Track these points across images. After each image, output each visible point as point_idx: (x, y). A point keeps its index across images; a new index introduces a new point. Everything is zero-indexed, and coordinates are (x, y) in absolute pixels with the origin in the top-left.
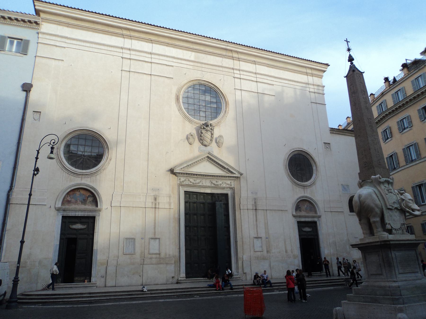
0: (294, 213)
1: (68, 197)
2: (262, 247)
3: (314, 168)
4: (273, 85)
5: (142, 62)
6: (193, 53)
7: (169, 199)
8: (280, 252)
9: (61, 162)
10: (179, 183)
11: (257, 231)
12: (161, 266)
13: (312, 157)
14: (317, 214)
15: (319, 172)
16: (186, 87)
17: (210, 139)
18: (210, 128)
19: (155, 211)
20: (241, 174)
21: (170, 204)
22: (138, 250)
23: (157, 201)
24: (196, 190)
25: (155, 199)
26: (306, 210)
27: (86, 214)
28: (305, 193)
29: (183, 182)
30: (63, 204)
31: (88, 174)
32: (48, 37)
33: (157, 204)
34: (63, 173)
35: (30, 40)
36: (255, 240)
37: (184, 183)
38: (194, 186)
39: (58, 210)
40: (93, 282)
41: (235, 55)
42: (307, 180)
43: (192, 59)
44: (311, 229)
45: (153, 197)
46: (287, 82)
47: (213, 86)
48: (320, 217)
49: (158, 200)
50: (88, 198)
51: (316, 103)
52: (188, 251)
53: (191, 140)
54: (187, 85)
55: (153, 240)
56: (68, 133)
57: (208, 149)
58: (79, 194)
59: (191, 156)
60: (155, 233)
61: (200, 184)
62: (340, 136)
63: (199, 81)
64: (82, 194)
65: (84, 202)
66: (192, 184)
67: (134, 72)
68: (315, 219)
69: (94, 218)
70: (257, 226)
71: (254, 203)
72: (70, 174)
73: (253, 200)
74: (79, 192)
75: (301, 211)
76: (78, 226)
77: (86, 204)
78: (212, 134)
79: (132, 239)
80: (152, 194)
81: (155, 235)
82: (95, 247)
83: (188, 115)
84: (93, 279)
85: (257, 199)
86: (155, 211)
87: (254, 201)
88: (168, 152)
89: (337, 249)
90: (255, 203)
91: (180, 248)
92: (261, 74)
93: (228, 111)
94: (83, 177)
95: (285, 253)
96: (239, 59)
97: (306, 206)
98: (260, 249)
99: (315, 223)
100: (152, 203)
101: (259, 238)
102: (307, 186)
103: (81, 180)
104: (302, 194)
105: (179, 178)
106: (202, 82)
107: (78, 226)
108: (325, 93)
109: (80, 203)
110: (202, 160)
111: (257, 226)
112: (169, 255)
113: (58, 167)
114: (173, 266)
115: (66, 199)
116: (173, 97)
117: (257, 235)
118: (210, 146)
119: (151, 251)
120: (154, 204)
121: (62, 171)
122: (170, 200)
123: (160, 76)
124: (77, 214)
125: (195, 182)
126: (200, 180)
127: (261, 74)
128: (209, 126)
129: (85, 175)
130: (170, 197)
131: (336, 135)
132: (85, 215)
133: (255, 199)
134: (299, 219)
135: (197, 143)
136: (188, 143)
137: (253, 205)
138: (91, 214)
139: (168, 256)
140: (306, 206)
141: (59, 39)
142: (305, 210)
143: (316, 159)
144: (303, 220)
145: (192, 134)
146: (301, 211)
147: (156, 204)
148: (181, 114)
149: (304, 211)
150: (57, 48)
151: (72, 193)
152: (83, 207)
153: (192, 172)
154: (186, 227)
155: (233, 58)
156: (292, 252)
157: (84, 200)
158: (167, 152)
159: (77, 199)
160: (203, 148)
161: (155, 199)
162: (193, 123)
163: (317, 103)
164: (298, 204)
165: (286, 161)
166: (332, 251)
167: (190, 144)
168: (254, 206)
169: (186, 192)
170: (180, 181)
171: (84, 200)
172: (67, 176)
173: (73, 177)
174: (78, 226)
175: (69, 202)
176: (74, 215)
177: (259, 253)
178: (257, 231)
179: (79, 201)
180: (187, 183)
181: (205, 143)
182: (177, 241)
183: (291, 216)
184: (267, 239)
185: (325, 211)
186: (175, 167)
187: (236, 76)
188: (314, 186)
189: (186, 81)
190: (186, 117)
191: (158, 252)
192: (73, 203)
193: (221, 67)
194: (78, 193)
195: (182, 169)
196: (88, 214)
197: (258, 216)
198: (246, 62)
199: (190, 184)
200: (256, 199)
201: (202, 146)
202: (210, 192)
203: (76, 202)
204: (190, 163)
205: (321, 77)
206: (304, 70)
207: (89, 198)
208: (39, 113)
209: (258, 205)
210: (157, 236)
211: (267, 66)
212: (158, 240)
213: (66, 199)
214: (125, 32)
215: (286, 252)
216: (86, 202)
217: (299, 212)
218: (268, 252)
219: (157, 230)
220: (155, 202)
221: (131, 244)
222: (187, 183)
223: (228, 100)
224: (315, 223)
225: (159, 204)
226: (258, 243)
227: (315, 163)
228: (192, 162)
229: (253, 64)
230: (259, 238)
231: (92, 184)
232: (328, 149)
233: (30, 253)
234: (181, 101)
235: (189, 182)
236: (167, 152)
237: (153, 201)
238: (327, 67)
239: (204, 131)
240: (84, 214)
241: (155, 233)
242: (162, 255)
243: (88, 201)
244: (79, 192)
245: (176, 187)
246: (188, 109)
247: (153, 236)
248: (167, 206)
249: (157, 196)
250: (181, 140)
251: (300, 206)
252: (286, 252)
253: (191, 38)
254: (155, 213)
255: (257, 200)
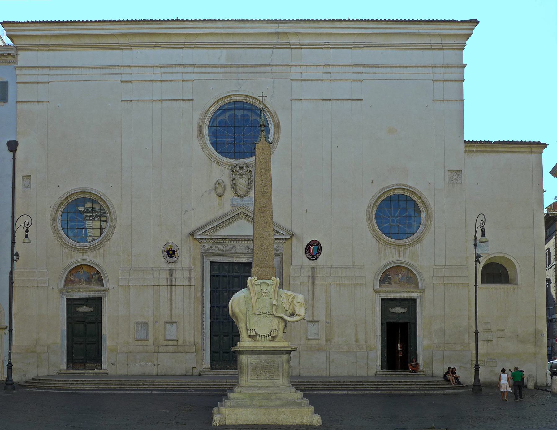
0: (377, 287)
1: (70, 276)
2: (318, 334)
3: (424, 215)
4: (362, 81)
5: (149, 83)
6: (225, 51)
7: (188, 274)
8: (345, 342)
9: (59, 236)
10: (203, 251)
11: (313, 313)
12: (179, 354)
13: (420, 198)
14: (418, 288)
15: (431, 221)
16: (213, 110)
17: (247, 187)
18: (246, 170)
19: (171, 289)
20: (293, 235)
21: (190, 279)
22: (151, 336)
23: (174, 277)
24: (226, 260)
25: (171, 275)
26: (399, 281)
27: (91, 295)
28: (400, 256)
29: (208, 249)
30: (66, 284)
31: (90, 248)
32: (26, 71)
33: (174, 280)
34: (63, 249)
35: (7, 81)
36: (309, 325)
37: (210, 251)
38: (223, 254)
39: (61, 291)
40: (104, 369)
41: (294, 40)
42: (407, 235)
43: (223, 61)
44: (406, 309)
45: (168, 272)
46: (388, 70)
47: (255, 101)
48: (422, 292)
49: (175, 275)
50: (92, 276)
51: (443, 100)
52: (216, 338)
53: (220, 190)
54: (214, 107)
55: (169, 324)
56: (63, 198)
57: (245, 199)
58: (82, 272)
59: (220, 212)
60: (171, 315)
61: (232, 252)
62: (486, 154)
63: (234, 97)
64: (86, 272)
65: (89, 281)
66: (220, 252)
67: (138, 100)
68: (413, 296)
69: (100, 299)
70: (313, 306)
71: (310, 274)
72: (69, 249)
73: (310, 270)
74: (82, 269)
75: (391, 284)
76: (85, 309)
77: (91, 283)
78: (249, 179)
79: (144, 323)
80: (168, 269)
81: (171, 318)
82: (104, 332)
83: (216, 153)
84: (104, 366)
85: (317, 268)
86: (171, 289)
87: (312, 271)
88: (188, 211)
89: (446, 339)
90: (313, 273)
91: (203, 335)
92: (339, 66)
93: (277, 139)
94: (84, 252)
95: (354, 343)
96: (301, 46)
97: (400, 275)
98: (316, 336)
99: (415, 300)
100: (167, 279)
101: (315, 322)
102: (406, 245)
103: (83, 255)
104: (396, 258)
105: (203, 245)
106: (238, 98)
107: (85, 309)
108: (464, 79)
109: (85, 283)
110: (236, 217)
111: (313, 306)
112: (189, 342)
113: (57, 242)
114: (194, 354)
115: (69, 279)
116: (195, 129)
117: (313, 318)
118: (248, 196)
119: (168, 338)
120: (170, 280)
121: (61, 247)
122: (190, 274)
123: (175, 100)
124: (82, 295)
125: (224, 249)
126: (232, 246)
127: (339, 66)
128: (245, 168)
129: (86, 249)
130: (190, 271)
131: (479, 153)
132: (90, 296)
133: (313, 268)
134: (384, 296)
135: (229, 194)
136: (216, 196)
137: (309, 276)
138: (96, 295)
139: (187, 344)
140: (400, 275)
141: (41, 71)
142: (398, 282)
143: (430, 201)
144: (392, 296)
145: (220, 182)
146: (391, 284)
147: (171, 281)
148: (206, 153)
149: (395, 283)
150: (40, 84)
151: (74, 271)
152: (86, 287)
153: (219, 236)
154: (212, 307)
155: (289, 46)
156: (366, 342)
157: (88, 278)
158: (186, 211)
159: (81, 278)
160: (238, 200)
161: (171, 275)
162: (222, 165)
163: (446, 100)
164: (387, 273)
165: (371, 208)
166: (436, 341)
167: (220, 196)
168: (310, 277)
169: (212, 264)
170: (205, 248)
171: (88, 278)
172: (67, 252)
173: (73, 253)
174: (85, 309)
175: (72, 282)
176: (79, 297)
177: (313, 342)
178: (313, 313)
179: (83, 280)
180: (214, 251)
181: (240, 192)
182: (200, 326)
183: (370, 290)
184: (327, 324)
185: (433, 283)
186: (195, 231)
187: (294, 76)
188: (418, 246)
189: (212, 100)
190: (211, 157)
191: (175, 338)
192: (77, 283)
193: (268, 66)
194: (81, 271)
195: (205, 232)
196: (93, 295)
197: (315, 293)
198: (313, 48)
199: (217, 252)
200: (314, 268)
201: (236, 197)
202: (246, 262)
203: (80, 282)
204: (216, 224)
205: (462, 47)
206: (427, 40)
207: (94, 276)
208: (29, 178)
209: (317, 276)
210: (174, 320)
211: (352, 48)
212: (175, 324)
213: (69, 279)
214: (122, 40)
215: (357, 341)
216: (91, 281)
217: (389, 285)
218: (327, 340)
219: (173, 313)
220: (171, 278)
221: (143, 329)
222: (214, 250)
223: (278, 120)
224: (415, 300)
225: (175, 280)
226: (312, 330)
227: (426, 206)
228: (220, 222)
229: (327, 48)
230: (315, 322)
231: (95, 260)
232: (455, 181)
233: (38, 338)
234: (206, 133)
235: (216, 249)
236: (186, 211)
237: (168, 277)
238: (473, 27)
239: (237, 177)
240: (89, 295)
241: (171, 315)
242: (181, 342)
243: (93, 280)
244: (82, 269)
245: (199, 257)
246: (215, 145)
247: (169, 320)
248: (186, 283)
249: (173, 270)
250: (206, 191)
251: (389, 275)
252: (357, 341)
253: (217, 28)
254: (171, 292)
255: (315, 269)
